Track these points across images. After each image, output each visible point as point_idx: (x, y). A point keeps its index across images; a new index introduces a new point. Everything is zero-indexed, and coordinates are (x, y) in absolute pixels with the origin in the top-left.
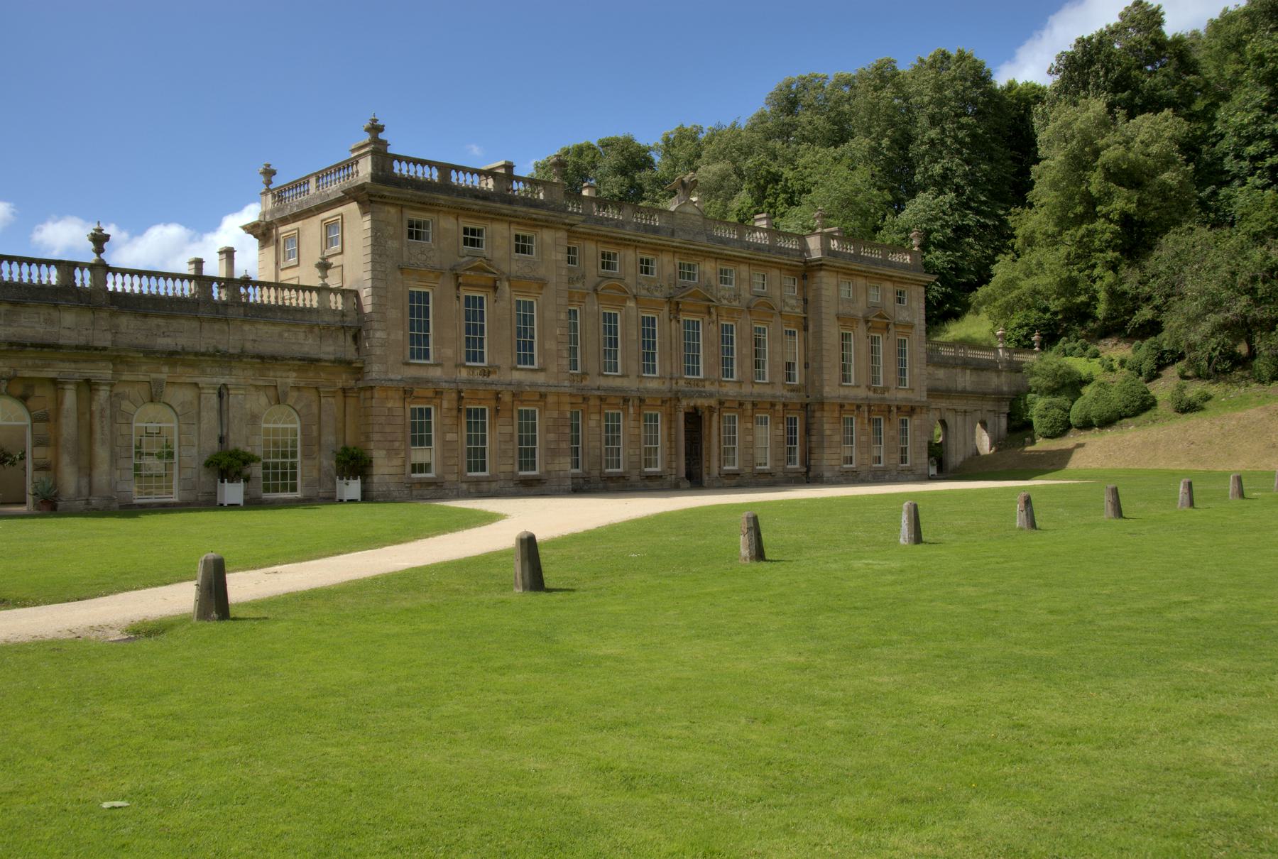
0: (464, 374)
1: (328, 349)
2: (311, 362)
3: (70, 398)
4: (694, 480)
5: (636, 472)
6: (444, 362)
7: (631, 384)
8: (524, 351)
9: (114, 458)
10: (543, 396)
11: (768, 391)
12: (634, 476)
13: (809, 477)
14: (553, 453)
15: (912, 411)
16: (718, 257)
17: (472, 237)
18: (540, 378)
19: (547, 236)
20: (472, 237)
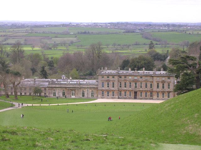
0: (106, 89)
1: (96, 87)
2: (94, 88)
3: (77, 91)
4: (135, 98)
5: (128, 97)
6: (106, 88)
7: (128, 89)
8: (113, 87)
9: (80, 94)
10: (115, 90)
11: (147, 89)
12: (128, 97)
13: (152, 99)
14: (115, 96)
15: (170, 92)
16: (139, 76)
17: (108, 77)
18: (114, 89)
19: (115, 77)
20: (108, 77)
